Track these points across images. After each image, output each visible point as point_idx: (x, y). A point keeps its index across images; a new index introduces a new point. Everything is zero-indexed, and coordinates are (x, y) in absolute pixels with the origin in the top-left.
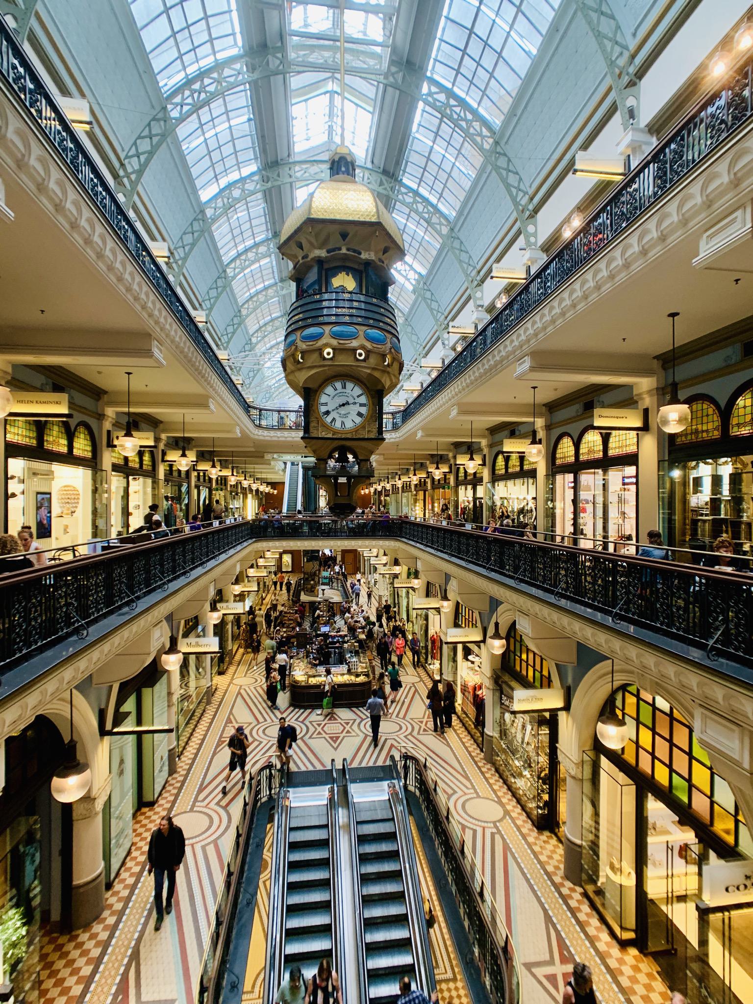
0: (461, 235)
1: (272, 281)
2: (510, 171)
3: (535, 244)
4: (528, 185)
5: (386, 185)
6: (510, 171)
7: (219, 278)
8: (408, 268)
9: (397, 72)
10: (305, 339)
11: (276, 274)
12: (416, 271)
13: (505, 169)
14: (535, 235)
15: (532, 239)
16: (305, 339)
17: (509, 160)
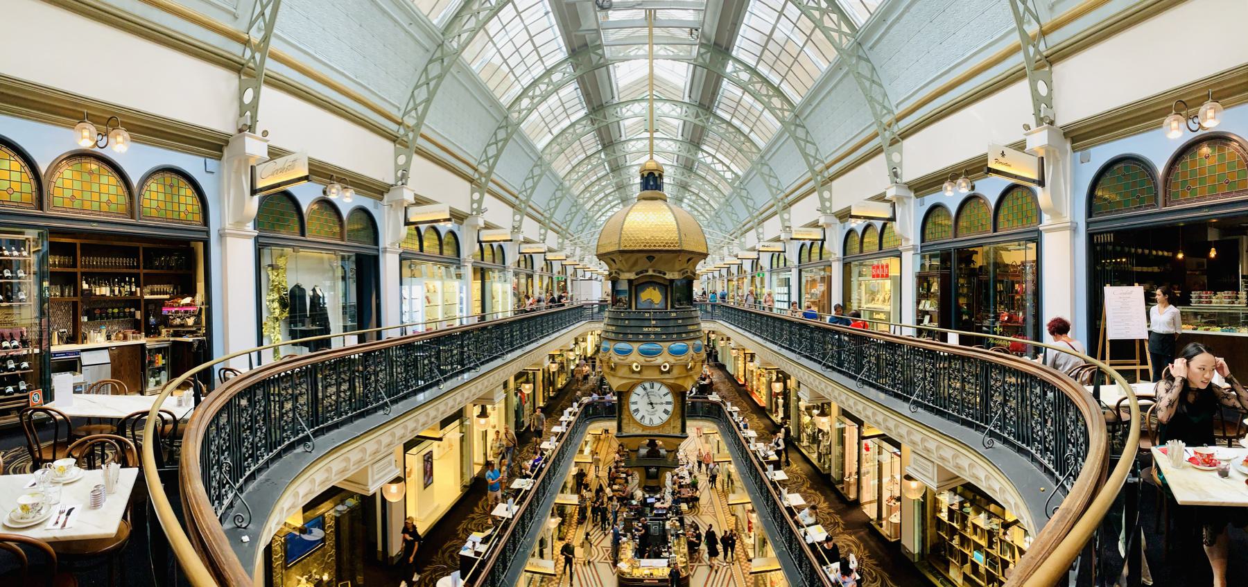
0: (769, 163)
1: (604, 173)
2: (808, 142)
3: (830, 208)
4: (824, 157)
5: (702, 117)
6: (808, 142)
7: (557, 190)
8: (725, 169)
9: (705, 53)
10: (619, 352)
11: (607, 168)
12: (733, 172)
13: (804, 140)
14: (830, 200)
15: (828, 204)
16: (619, 352)
17: (807, 132)
